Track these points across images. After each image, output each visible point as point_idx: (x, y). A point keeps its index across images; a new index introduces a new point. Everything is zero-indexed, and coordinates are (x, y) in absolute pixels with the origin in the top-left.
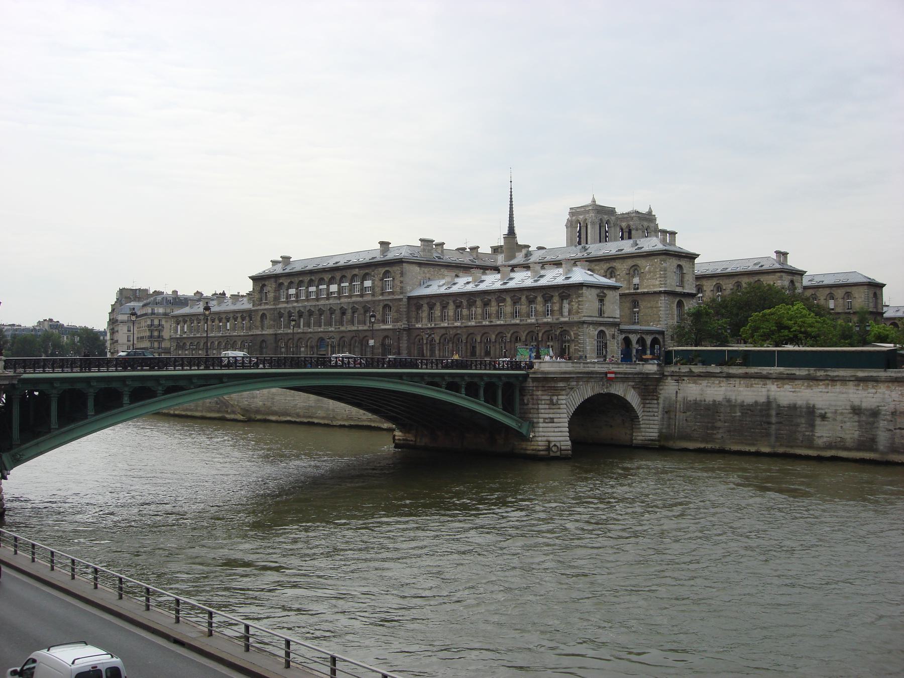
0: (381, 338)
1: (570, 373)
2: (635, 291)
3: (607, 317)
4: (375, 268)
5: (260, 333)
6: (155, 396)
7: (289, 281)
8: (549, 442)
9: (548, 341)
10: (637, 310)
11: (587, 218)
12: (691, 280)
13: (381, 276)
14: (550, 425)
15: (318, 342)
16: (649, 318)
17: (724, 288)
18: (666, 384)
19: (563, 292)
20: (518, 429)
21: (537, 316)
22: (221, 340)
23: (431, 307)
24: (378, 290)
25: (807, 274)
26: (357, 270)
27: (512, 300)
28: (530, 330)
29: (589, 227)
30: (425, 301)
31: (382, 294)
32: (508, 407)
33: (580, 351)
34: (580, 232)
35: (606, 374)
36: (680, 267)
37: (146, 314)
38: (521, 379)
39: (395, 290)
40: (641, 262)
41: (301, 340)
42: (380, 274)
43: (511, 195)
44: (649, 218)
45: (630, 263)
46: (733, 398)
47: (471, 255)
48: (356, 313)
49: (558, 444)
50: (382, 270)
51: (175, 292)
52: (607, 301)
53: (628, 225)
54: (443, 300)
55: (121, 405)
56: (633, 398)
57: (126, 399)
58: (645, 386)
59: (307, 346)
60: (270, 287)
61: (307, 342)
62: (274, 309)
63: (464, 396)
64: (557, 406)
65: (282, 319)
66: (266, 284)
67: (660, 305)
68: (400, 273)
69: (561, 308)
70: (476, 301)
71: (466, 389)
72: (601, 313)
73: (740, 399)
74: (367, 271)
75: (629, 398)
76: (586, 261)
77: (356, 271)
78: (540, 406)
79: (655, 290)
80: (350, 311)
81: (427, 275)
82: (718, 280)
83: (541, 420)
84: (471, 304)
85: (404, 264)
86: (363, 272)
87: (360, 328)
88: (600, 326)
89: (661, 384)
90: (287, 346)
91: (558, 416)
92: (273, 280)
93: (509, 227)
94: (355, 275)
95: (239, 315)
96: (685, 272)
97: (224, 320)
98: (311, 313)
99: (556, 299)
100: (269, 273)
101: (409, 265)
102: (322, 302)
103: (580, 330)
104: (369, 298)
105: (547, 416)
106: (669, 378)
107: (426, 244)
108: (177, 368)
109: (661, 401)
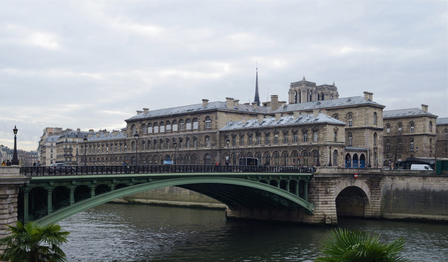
0: (204, 155)
1: (337, 174)
2: (350, 127)
3: (338, 142)
4: (201, 115)
5: (131, 152)
6: (110, 191)
7: (148, 122)
8: (325, 215)
9: (305, 156)
10: (351, 138)
11: (301, 88)
12: (381, 121)
13: (204, 119)
14: (325, 205)
15: (165, 157)
16: (358, 143)
17: (391, 126)
18: (385, 181)
19: (315, 128)
20: (307, 208)
21: (298, 142)
22: (107, 156)
23: (234, 137)
24: (202, 127)
25: (438, 118)
27: (283, 132)
28: (294, 150)
29: (302, 93)
30: (230, 133)
31: (205, 130)
32: (302, 195)
33: (324, 162)
34: (296, 96)
36: (375, 113)
37: (62, 142)
38: (309, 178)
39: (212, 127)
40: (353, 111)
41: (155, 156)
42: (203, 118)
43: (257, 76)
44: (333, 88)
45: (347, 111)
46: (428, 188)
47: (253, 107)
48: (189, 141)
49: (330, 217)
50: (205, 116)
51: (79, 130)
52: (339, 132)
53: (322, 92)
54: (241, 133)
55: (90, 196)
56: (366, 189)
57: (93, 193)
58: (372, 182)
59: (159, 160)
60: (138, 126)
61: (159, 158)
63: (279, 188)
64: (330, 194)
65: (144, 145)
66: (135, 124)
67: (365, 135)
68: (216, 118)
69: (313, 138)
70: (261, 133)
71: (280, 184)
72: (336, 139)
73: (432, 189)
74: (195, 117)
75: (364, 189)
76: (326, 110)
77: (189, 117)
78: (320, 194)
79: (362, 126)
80: (185, 139)
81: (230, 119)
82: (388, 122)
83: (320, 203)
84: (258, 135)
85: (218, 112)
86: (192, 117)
87: (191, 149)
88: (335, 147)
89: (382, 180)
90: (147, 160)
91: (330, 200)
92: (139, 122)
93: (256, 94)
94: (188, 119)
95: (118, 143)
96: (378, 116)
97: (109, 145)
98: (161, 141)
99: (310, 132)
100: (136, 118)
101: (220, 113)
102: (168, 134)
103: (324, 150)
104: (196, 132)
105: (323, 200)
106: (387, 177)
107: (230, 100)
108: (132, 172)
109: (381, 191)
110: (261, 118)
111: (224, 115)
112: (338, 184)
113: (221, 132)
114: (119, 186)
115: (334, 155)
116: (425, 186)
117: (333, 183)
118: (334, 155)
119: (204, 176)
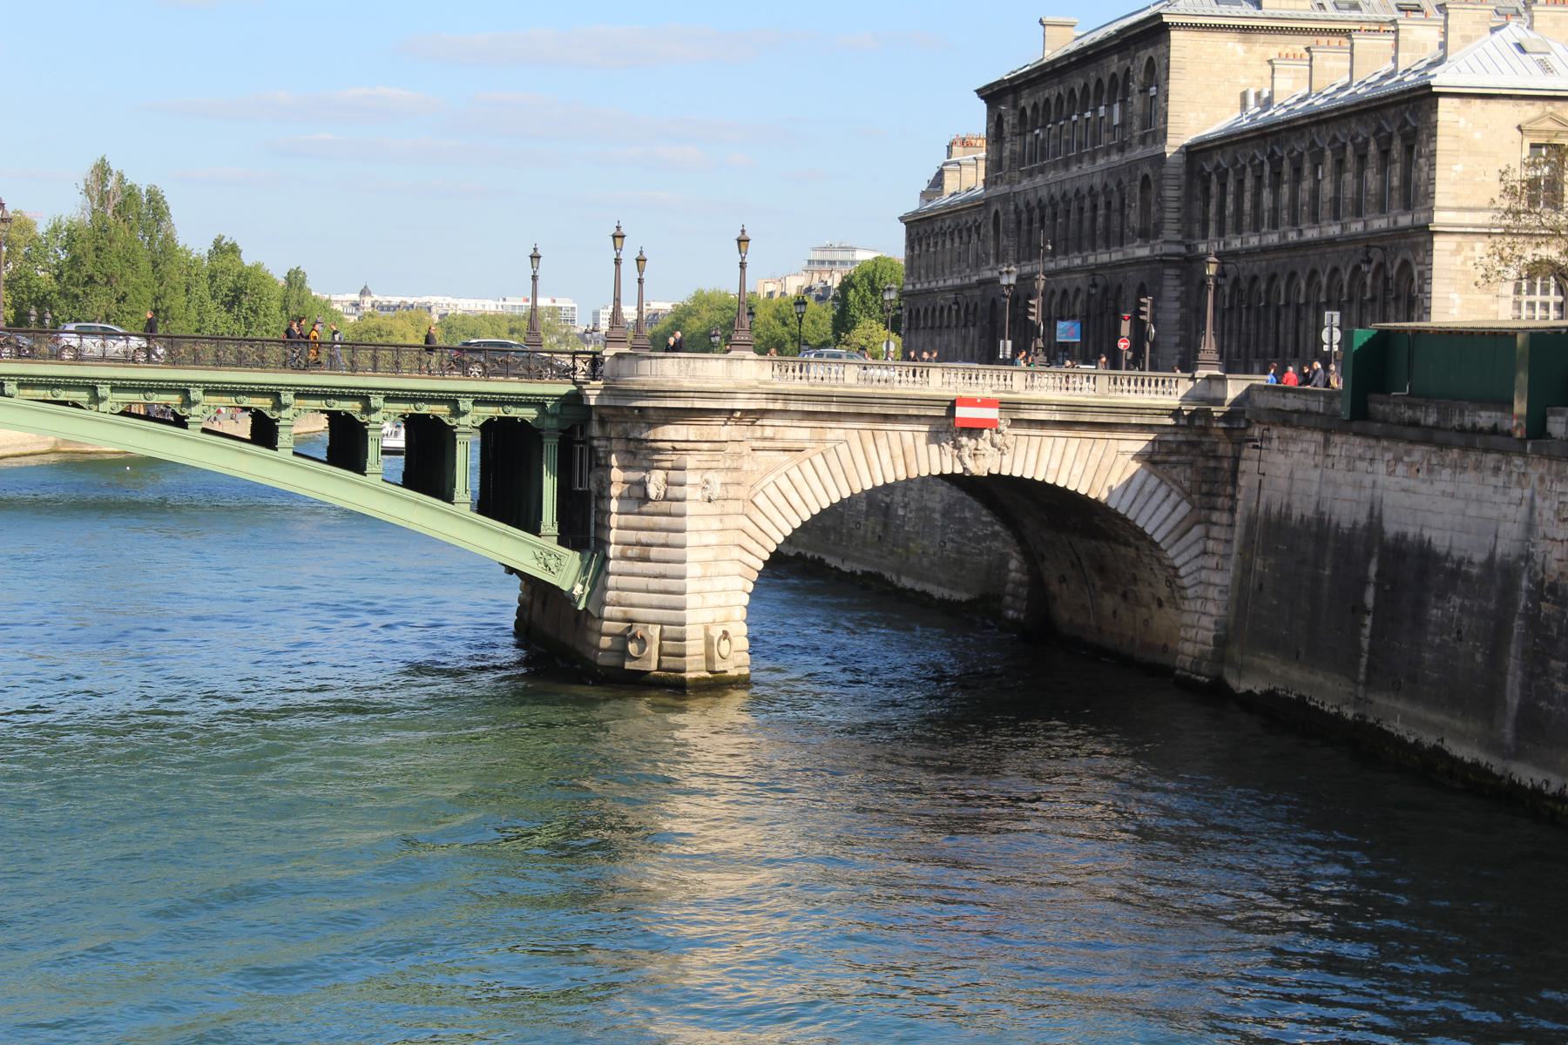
7: (1032, 102)
13: (1142, 77)
26: (1115, 57)
35: (952, 406)
46: (1325, 508)
50: (1144, 55)
60: (1010, 119)
62: (1005, 198)
91: (660, 537)
105: (631, 536)
110: (1327, 64)
111: (1231, 46)
112: (819, 461)
113: (1196, 152)
115: (1525, 299)
116: (1328, 492)
117: (677, 445)
118: (1525, 299)
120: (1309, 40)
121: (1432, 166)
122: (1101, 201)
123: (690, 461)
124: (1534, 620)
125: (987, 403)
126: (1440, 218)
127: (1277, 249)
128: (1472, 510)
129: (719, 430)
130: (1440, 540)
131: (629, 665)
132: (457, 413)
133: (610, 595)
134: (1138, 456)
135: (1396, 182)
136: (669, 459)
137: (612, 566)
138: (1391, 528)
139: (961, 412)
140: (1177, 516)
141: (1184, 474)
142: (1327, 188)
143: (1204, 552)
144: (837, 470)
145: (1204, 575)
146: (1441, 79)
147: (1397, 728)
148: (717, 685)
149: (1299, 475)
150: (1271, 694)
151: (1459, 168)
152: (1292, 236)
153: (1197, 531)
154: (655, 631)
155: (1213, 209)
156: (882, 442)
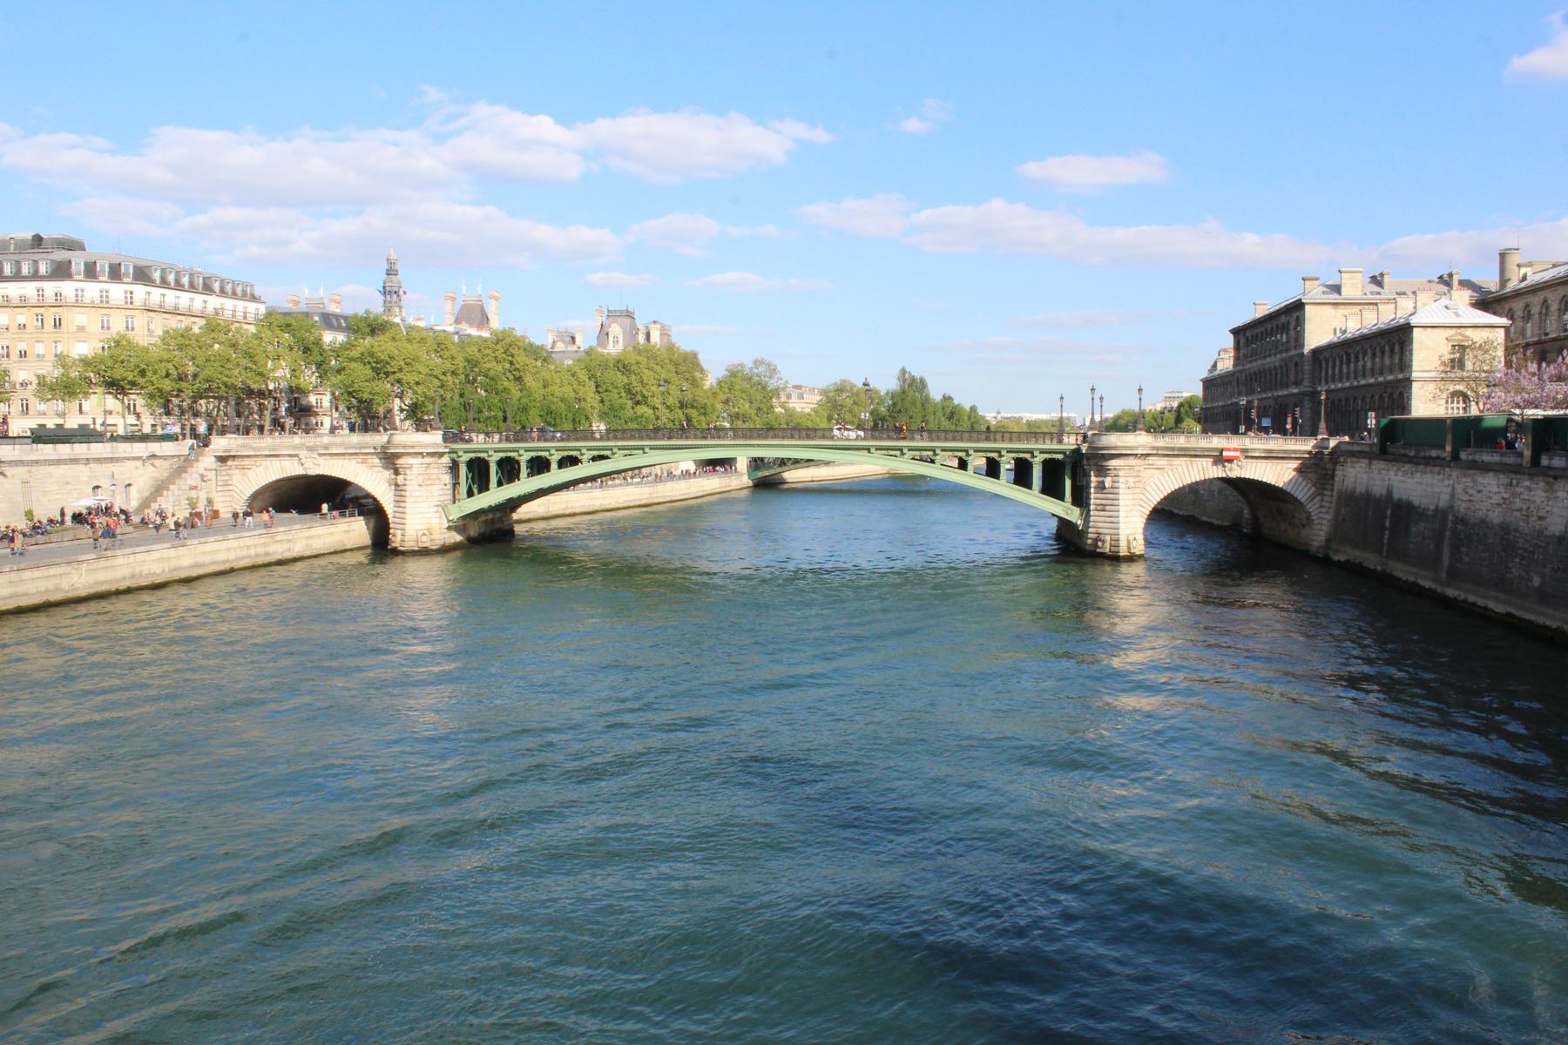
14: (1102, 513)
35: (1222, 450)
49: (1108, 538)
50: (1295, 315)
57: (554, 466)
60: (1243, 341)
62: (1241, 371)
91: (1110, 502)
105: (1099, 502)
111: (1329, 310)
112: (1170, 472)
113: (1316, 352)
114: (594, 459)
115: (1450, 406)
118: (1450, 406)
119: (759, 446)
120: (1360, 307)
121: (1411, 355)
122: (1279, 371)
123: (1121, 474)
124: (1454, 532)
125: (1235, 450)
126: (1414, 375)
127: (1349, 388)
128: (1429, 489)
129: (1132, 461)
130: (1416, 501)
131: (1098, 550)
132: (1033, 456)
133: (1091, 524)
134: (1295, 470)
135: (1397, 361)
136: (1113, 473)
137: (1092, 513)
138: (1396, 496)
139: (1225, 453)
140: (1310, 492)
141: (1313, 476)
142: (1369, 364)
143: (1321, 506)
144: (1177, 476)
145: (1321, 515)
146: (1414, 321)
147: (1398, 574)
148: (1131, 558)
149: (1359, 476)
150: (1348, 561)
151: (1422, 355)
152: (1355, 383)
153: (1318, 498)
154: (1108, 538)
155: (1323, 374)
156: (1195, 465)
